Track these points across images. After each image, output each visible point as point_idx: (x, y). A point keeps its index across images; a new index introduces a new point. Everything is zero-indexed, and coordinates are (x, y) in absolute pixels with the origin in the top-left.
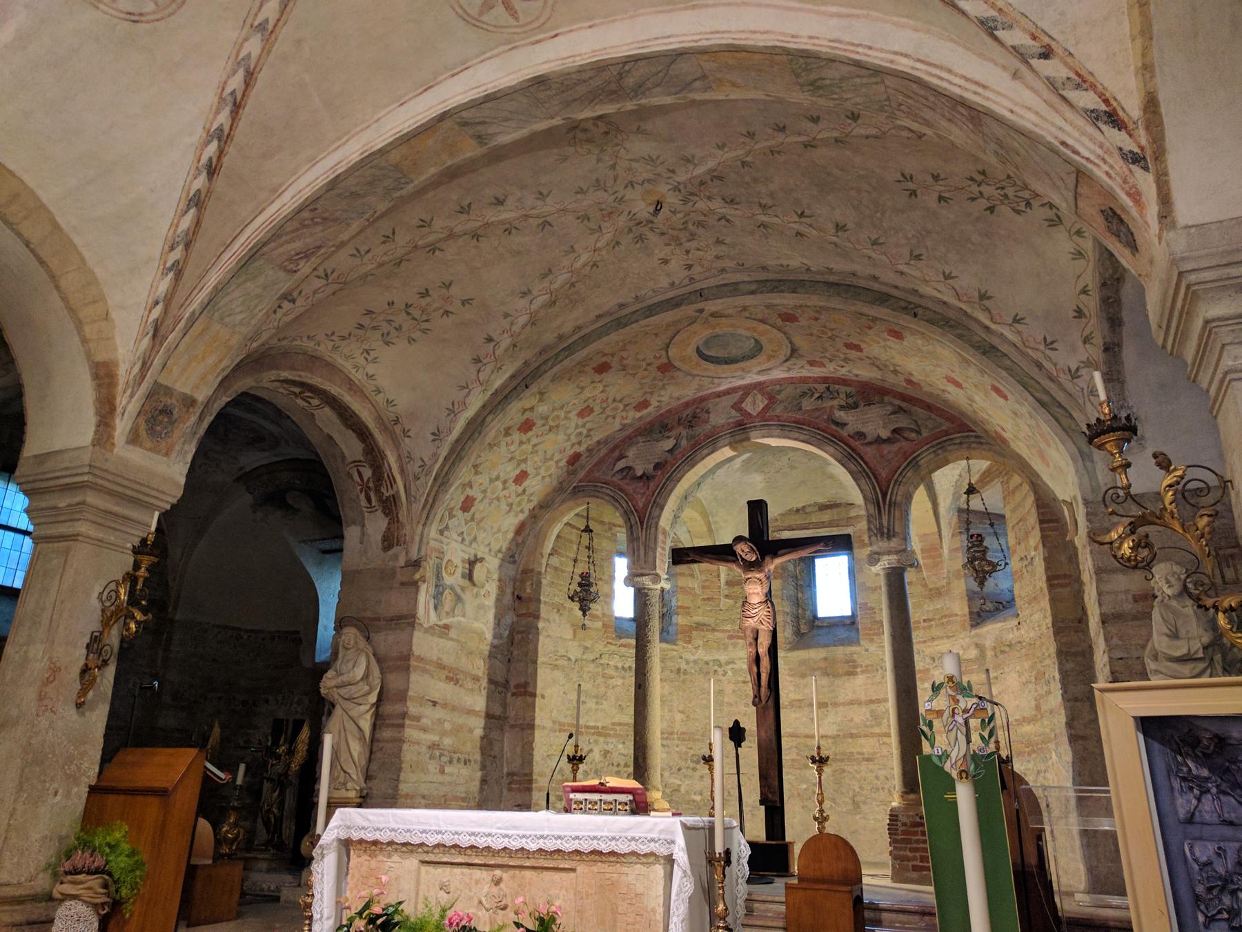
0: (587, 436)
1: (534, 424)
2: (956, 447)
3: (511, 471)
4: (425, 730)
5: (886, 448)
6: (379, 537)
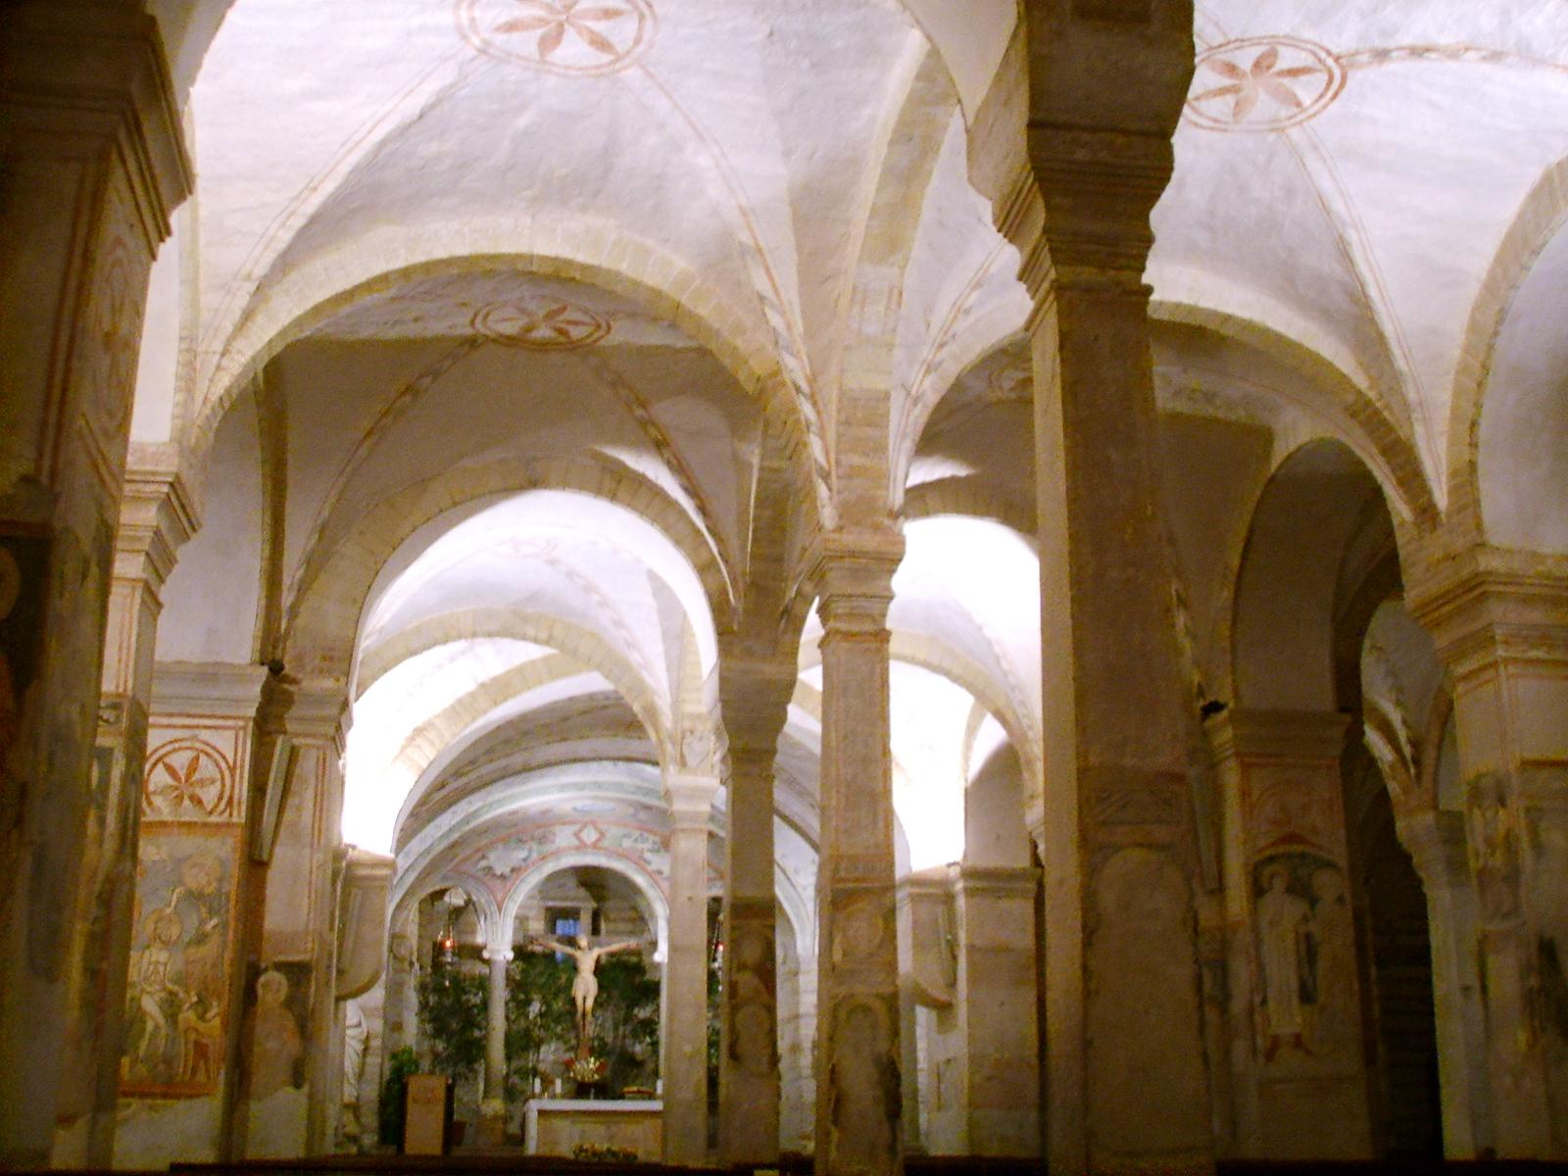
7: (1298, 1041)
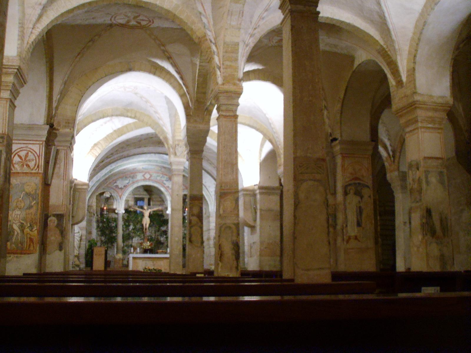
7: (356, 238)
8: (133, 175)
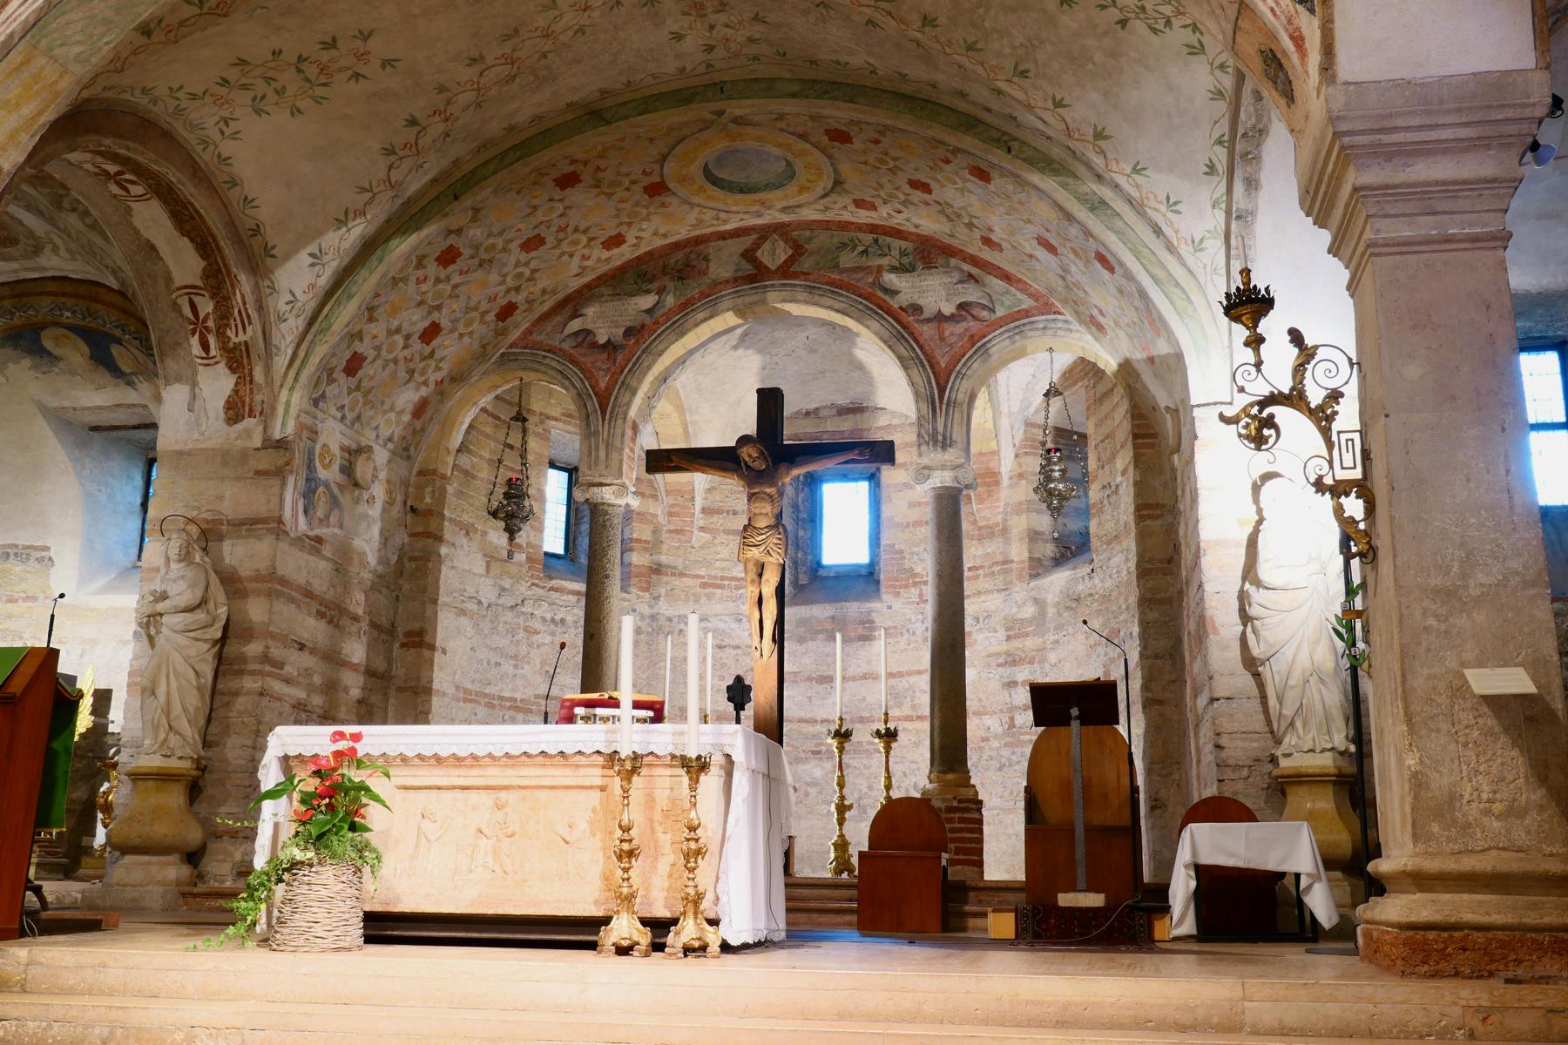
0: (529, 280)
1: (460, 254)
2: (1038, 333)
3: (416, 320)
4: (288, 681)
5: (950, 329)
6: (220, 404)
8: (680, 255)
